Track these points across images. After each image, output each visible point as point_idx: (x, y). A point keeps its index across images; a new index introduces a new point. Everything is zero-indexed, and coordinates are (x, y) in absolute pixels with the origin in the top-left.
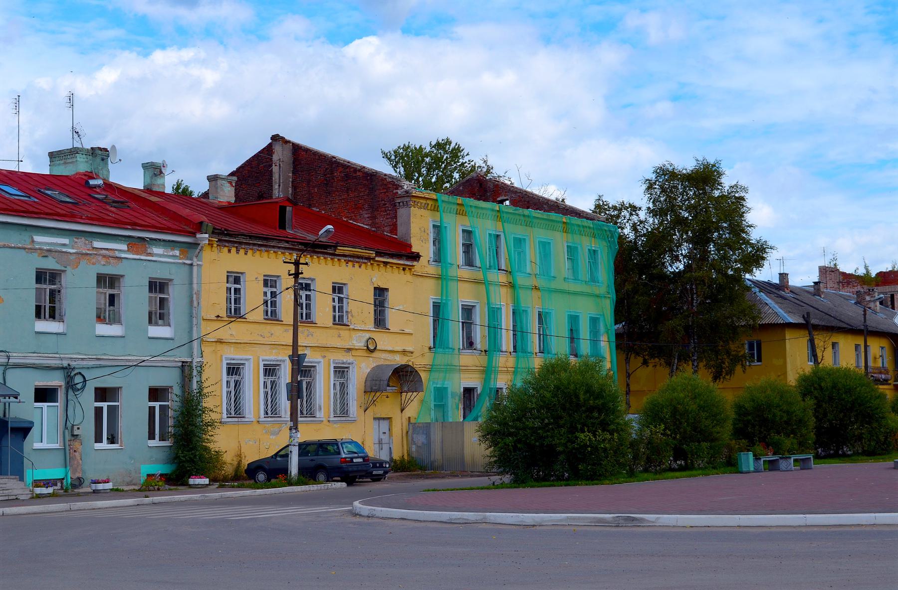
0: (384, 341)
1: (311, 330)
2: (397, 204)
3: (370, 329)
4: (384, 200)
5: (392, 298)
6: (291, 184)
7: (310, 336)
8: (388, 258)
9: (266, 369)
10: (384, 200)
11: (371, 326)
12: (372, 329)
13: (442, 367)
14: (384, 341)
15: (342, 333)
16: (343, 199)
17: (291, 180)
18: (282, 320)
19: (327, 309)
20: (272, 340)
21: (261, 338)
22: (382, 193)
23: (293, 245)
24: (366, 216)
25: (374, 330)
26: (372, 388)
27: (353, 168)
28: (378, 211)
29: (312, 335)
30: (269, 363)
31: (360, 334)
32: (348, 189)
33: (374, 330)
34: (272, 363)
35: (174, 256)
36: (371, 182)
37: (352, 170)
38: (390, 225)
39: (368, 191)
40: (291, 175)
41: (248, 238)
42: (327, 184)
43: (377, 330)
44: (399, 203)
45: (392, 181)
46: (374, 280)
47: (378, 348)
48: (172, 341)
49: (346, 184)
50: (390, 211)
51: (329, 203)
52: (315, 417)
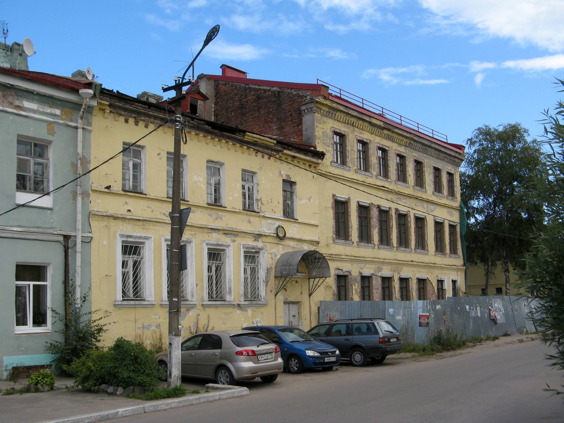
0: (292, 230)
1: (220, 213)
2: (303, 112)
3: (279, 218)
4: (290, 111)
5: (299, 189)
6: (213, 113)
7: (219, 219)
8: (295, 153)
10: (290, 111)
11: (279, 214)
12: (281, 218)
13: (344, 257)
14: (292, 230)
15: (252, 219)
16: (255, 117)
17: (213, 109)
18: (188, 200)
19: (237, 195)
22: (288, 105)
24: (274, 128)
25: (283, 218)
26: (282, 273)
27: (263, 89)
28: (285, 122)
29: (221, 219)
31: (270, 221)
32: (259, 108)
33: (283, 218)
35: (55, 115)
36: (279, 97)
37: (262, 91)
38: (296, 132)
39: (276, 106)
40: (213, 105)
41: (147, 107)
42: (241, 108)
43: (286, 219)
44: (304, 110)
45: (298, 94)
46: (283, 172)
47: (287, 235)
48: (49, 211)
49: (258, 104)
50: (296, 119)
51: (243, 122)
52: (225, 300)
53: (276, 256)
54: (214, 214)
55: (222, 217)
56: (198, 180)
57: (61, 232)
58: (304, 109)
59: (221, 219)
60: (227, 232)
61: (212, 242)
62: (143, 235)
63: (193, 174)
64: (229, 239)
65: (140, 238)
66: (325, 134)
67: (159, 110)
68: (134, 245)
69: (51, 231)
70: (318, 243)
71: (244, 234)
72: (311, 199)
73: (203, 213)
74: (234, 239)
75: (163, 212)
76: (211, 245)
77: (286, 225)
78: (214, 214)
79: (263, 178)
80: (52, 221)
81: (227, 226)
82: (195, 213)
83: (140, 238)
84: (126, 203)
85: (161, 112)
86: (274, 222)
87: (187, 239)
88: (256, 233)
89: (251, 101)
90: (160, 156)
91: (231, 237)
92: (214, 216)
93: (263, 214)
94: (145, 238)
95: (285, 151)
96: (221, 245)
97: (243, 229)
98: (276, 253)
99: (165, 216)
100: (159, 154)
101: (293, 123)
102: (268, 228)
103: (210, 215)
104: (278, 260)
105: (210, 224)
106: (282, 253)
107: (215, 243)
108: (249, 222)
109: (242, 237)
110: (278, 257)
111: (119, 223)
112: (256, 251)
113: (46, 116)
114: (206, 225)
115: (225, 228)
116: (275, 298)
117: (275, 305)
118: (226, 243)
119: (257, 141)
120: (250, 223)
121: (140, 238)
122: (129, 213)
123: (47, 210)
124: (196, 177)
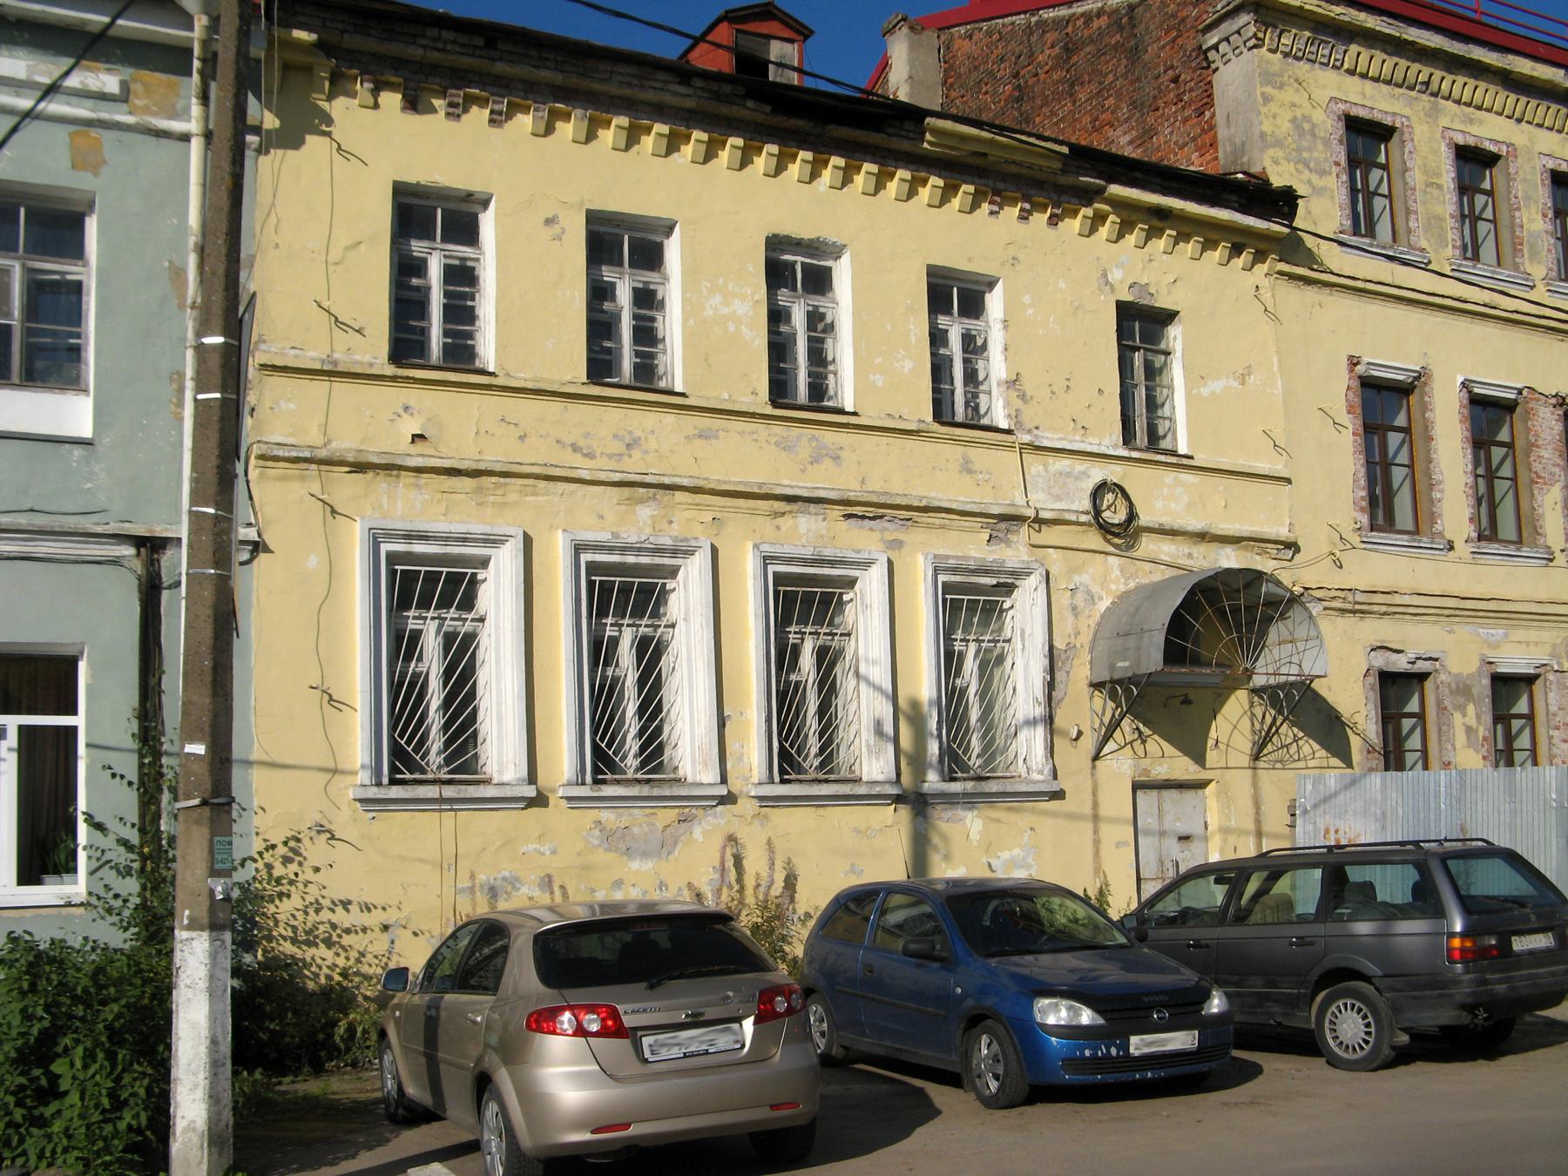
1: (830, 437)
2: (1212, 55)
3: (1103, 450)
9: (606, 589)
10: (1172, 67)
11: (1109, 439)
13: (1407, 600)
15: (981, 457)
16: (1062, 120)
20: (634, 465)
21: (577, 460)
22: (1164, 47)
23: (717, 97)
25: (1124, 453)
27: (1083, 15)
28: (1157, 109)
29: (836, 458)
30: (615, 558)
31: (1061, 464)
32: (1072, 86)
34: (631, 559)
36: (1134, 26)
37: (1080, 23)
38: (1194, 139)
39: (1124, 62)
41: (479, 41)
42: (1019, 100)
44: (1216, 47)
46: (1116, 275)
47: (1144, 519)
50: (1191, 90)
53: (1092, 599)
54: (804, 440)
55: (841, 453)
56: (725, 311)
57: (127, 525)
58: (1215, 40)
59: (836, 458)
60: (858, 509)
61: (787, 550)
62: (477, 528)
63: (705, 292)
64: (876, 535)
65: (465, 540)
66: (1306, 126)
67: (533, 53)
68: (445, 570)
69: (88, 524)
70: (1293, 546)
71: (943, 515)
72: (1249, 375)
73: (755, 436)
74: (895, 536)
75: (568, 439)
76: (790, 560)
77: (1138, 480)
78: (804, 440)
79: (1027, 299)
80: (89, 485)
81: (864, 488)
82: (717, 438)
83: (465, 540)
84: (406, 408)
85: (547, 59)
86: (1079, 466)
87: (675, 539)
88: (996, 510)
89: (1047, 68)
90: (556, 229)
91: (883, 530)
92: (805, 451)
93: (1026, 438)
94: (486, 541)
95: (1116, 190)
96: (833, 563)
97: (940, 496)
98: (1095, 589)
99: (579, 455)
100: (549, 222)
101: (1184, 108)
102: (1056, 491)
103: (785, 446)
104: (1103, 616)
105: (786, 482)
106: (1122, 588)
107: (808, 552)
108: (967, 468)
109: (930, 527)
110: (1104, 605)
111: (380, 484)
112: (998, 585)
113: (68, 104)
114: (760, 485)
115: (852, 496)
116: (1094, 767)
117: (1095, 794)
118: (858, 552)
119: (985, 155)
120: (970, 472)
121: (464, 540)
122: (420, 447)
123: (67, 446)
124: (717, 300)
